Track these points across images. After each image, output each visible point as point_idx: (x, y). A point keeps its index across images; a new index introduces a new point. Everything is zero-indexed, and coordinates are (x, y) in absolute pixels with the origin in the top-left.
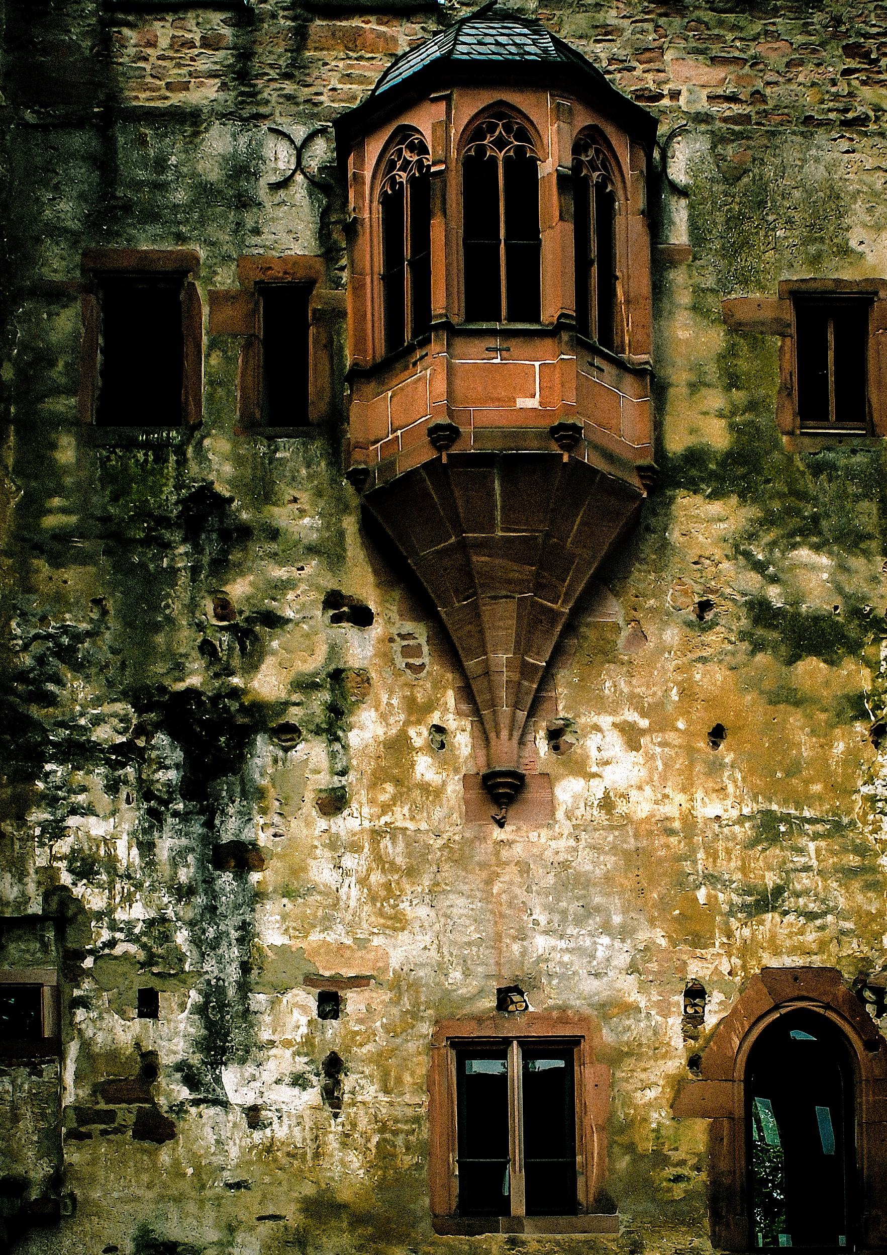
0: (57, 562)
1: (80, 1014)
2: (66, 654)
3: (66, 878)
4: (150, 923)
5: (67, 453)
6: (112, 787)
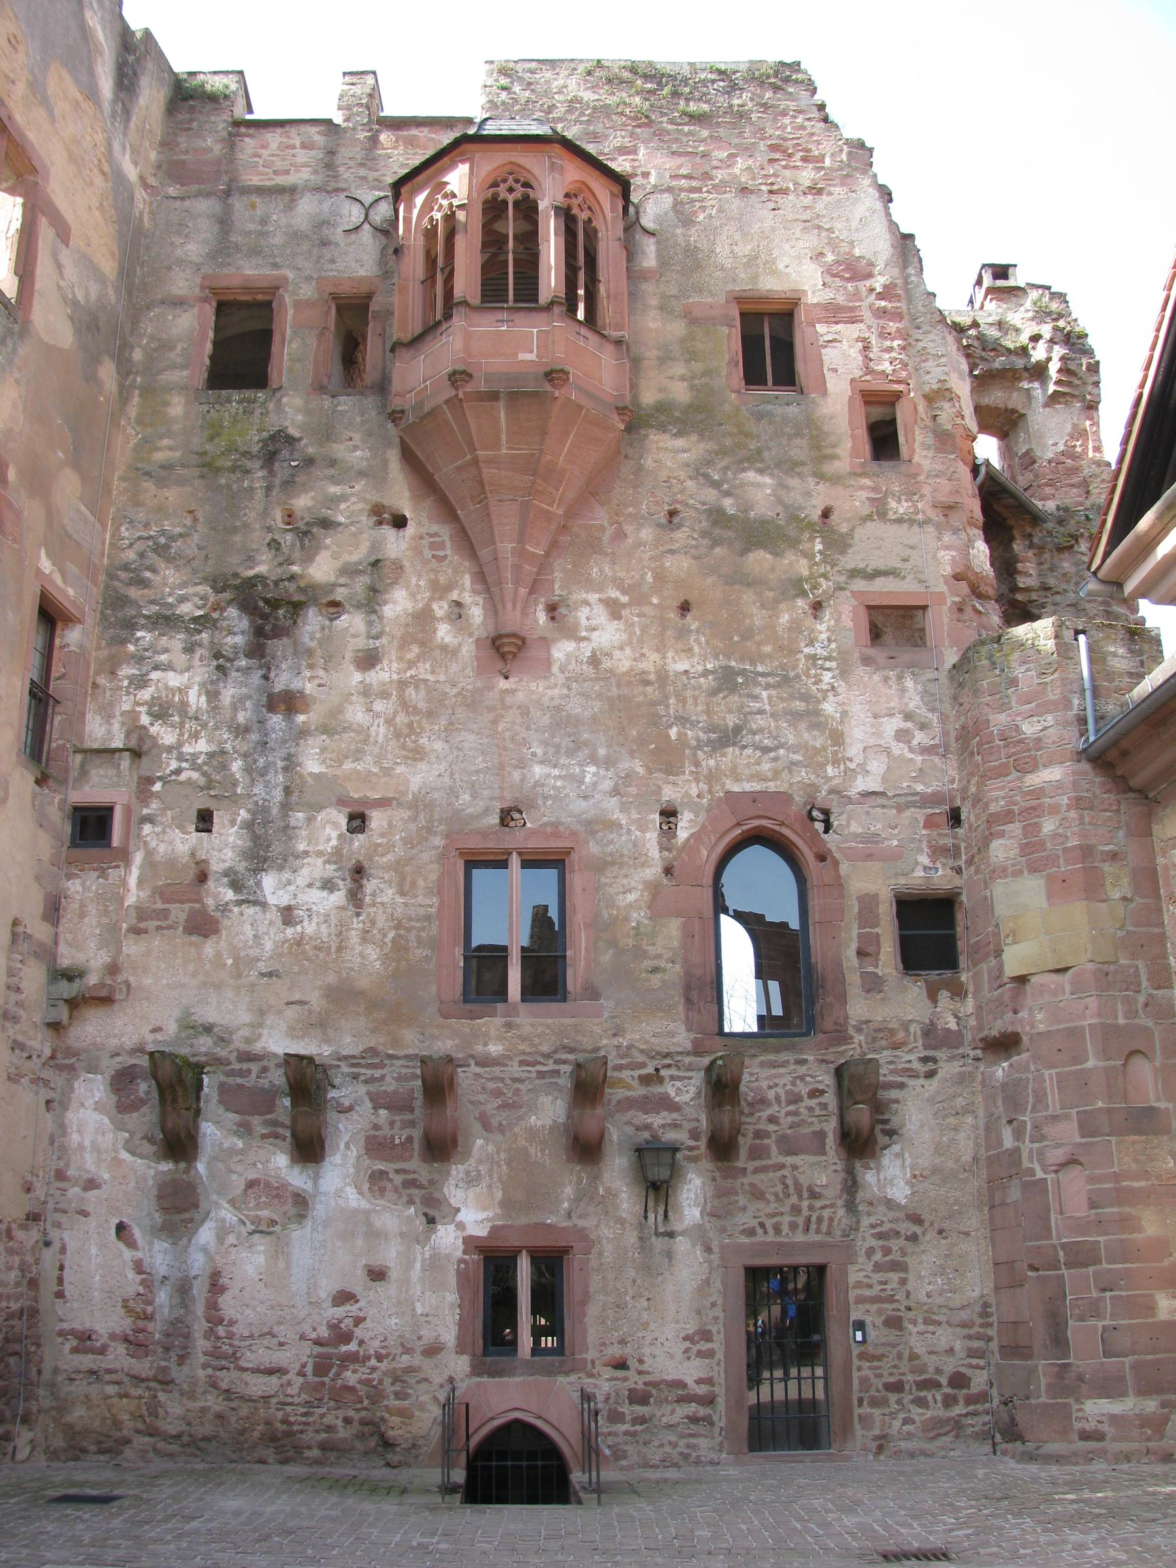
0: (162, 483)
1: (147, 829)
4: (211, 755)
5: (177, 407)
6: (189, 649)
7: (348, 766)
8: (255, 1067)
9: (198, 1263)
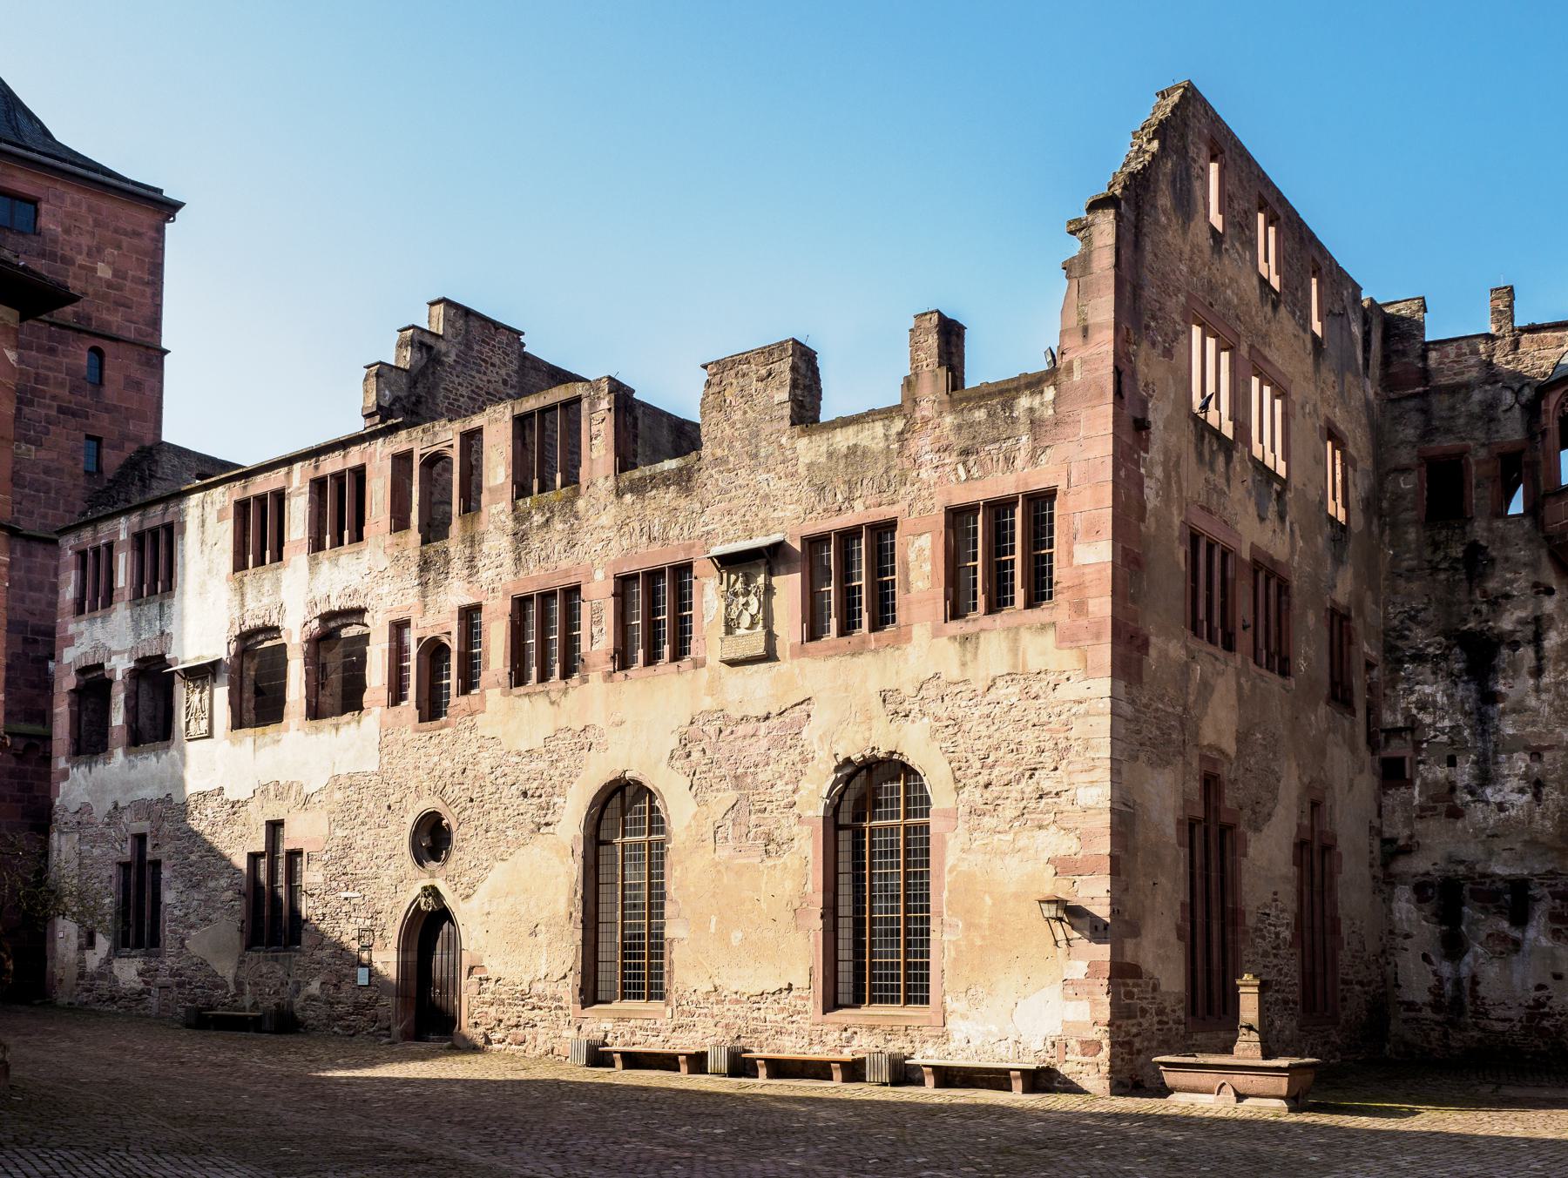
0: (1409, 580)
1: (1421, 767)
2: (1412, 618)
3: (1414, 711)
4: (1452, 728)
5: (1412, 535)
7: (1529, 729)
8: (1488, 881)
9: (1465, 971)
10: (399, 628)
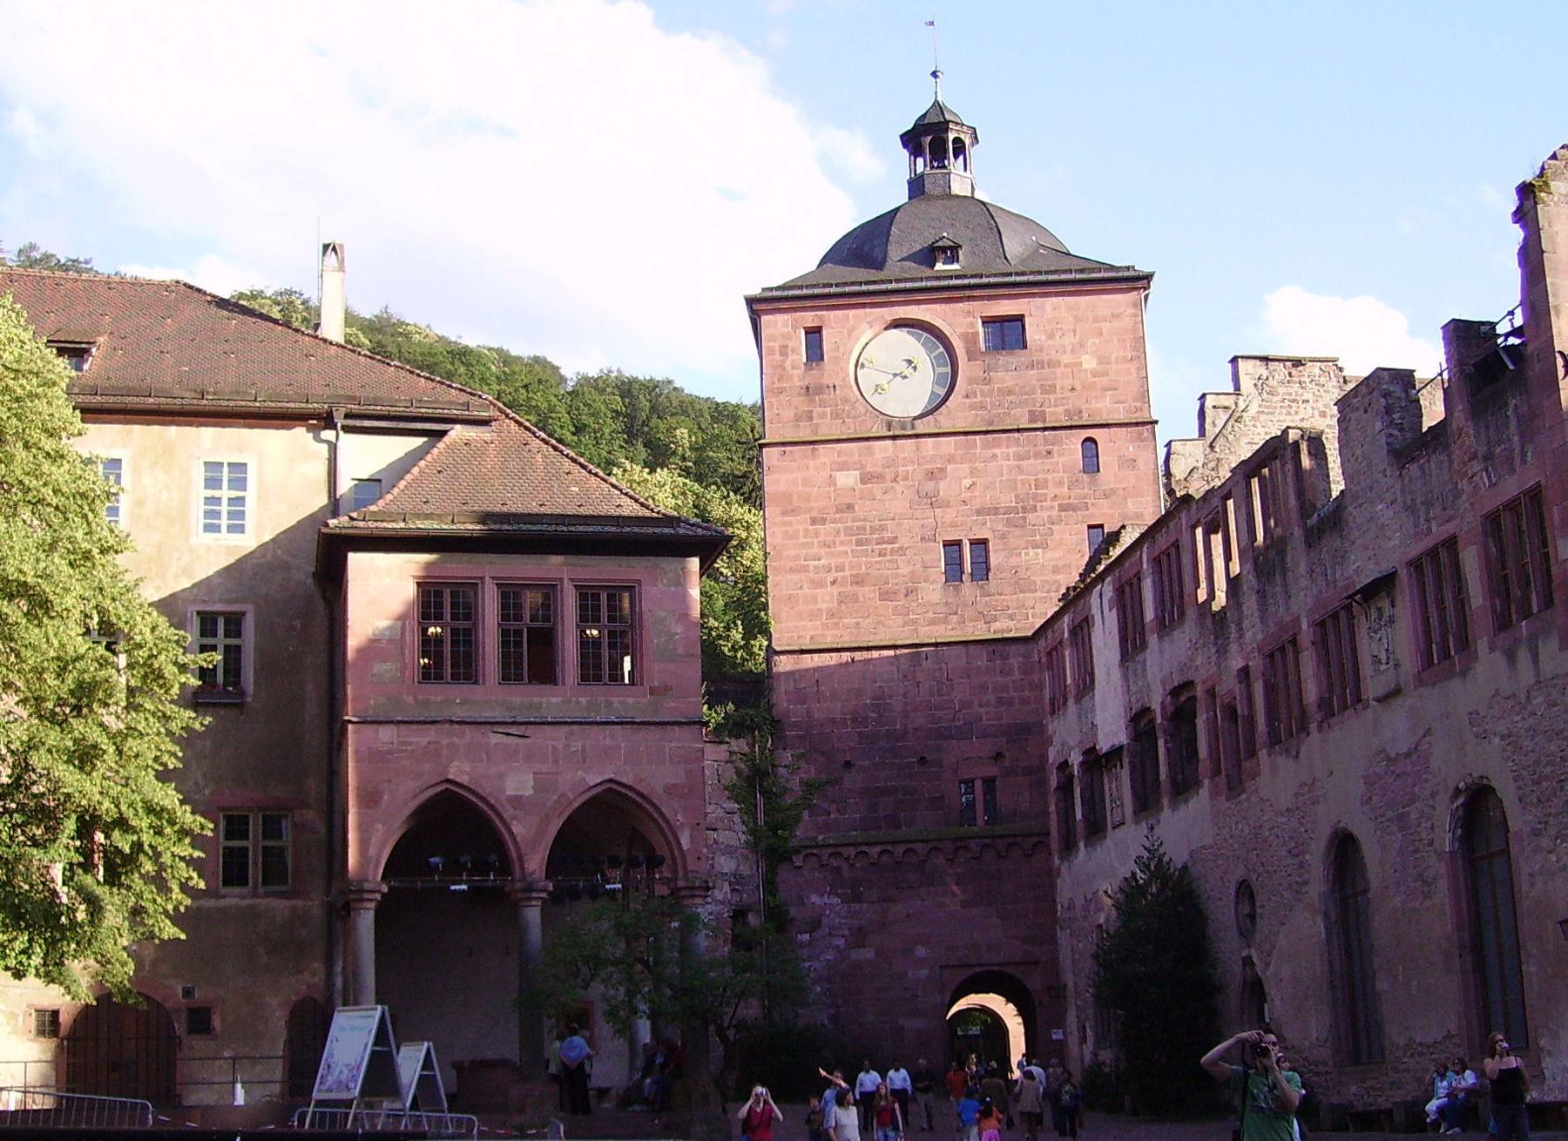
10: (1211, 693)
